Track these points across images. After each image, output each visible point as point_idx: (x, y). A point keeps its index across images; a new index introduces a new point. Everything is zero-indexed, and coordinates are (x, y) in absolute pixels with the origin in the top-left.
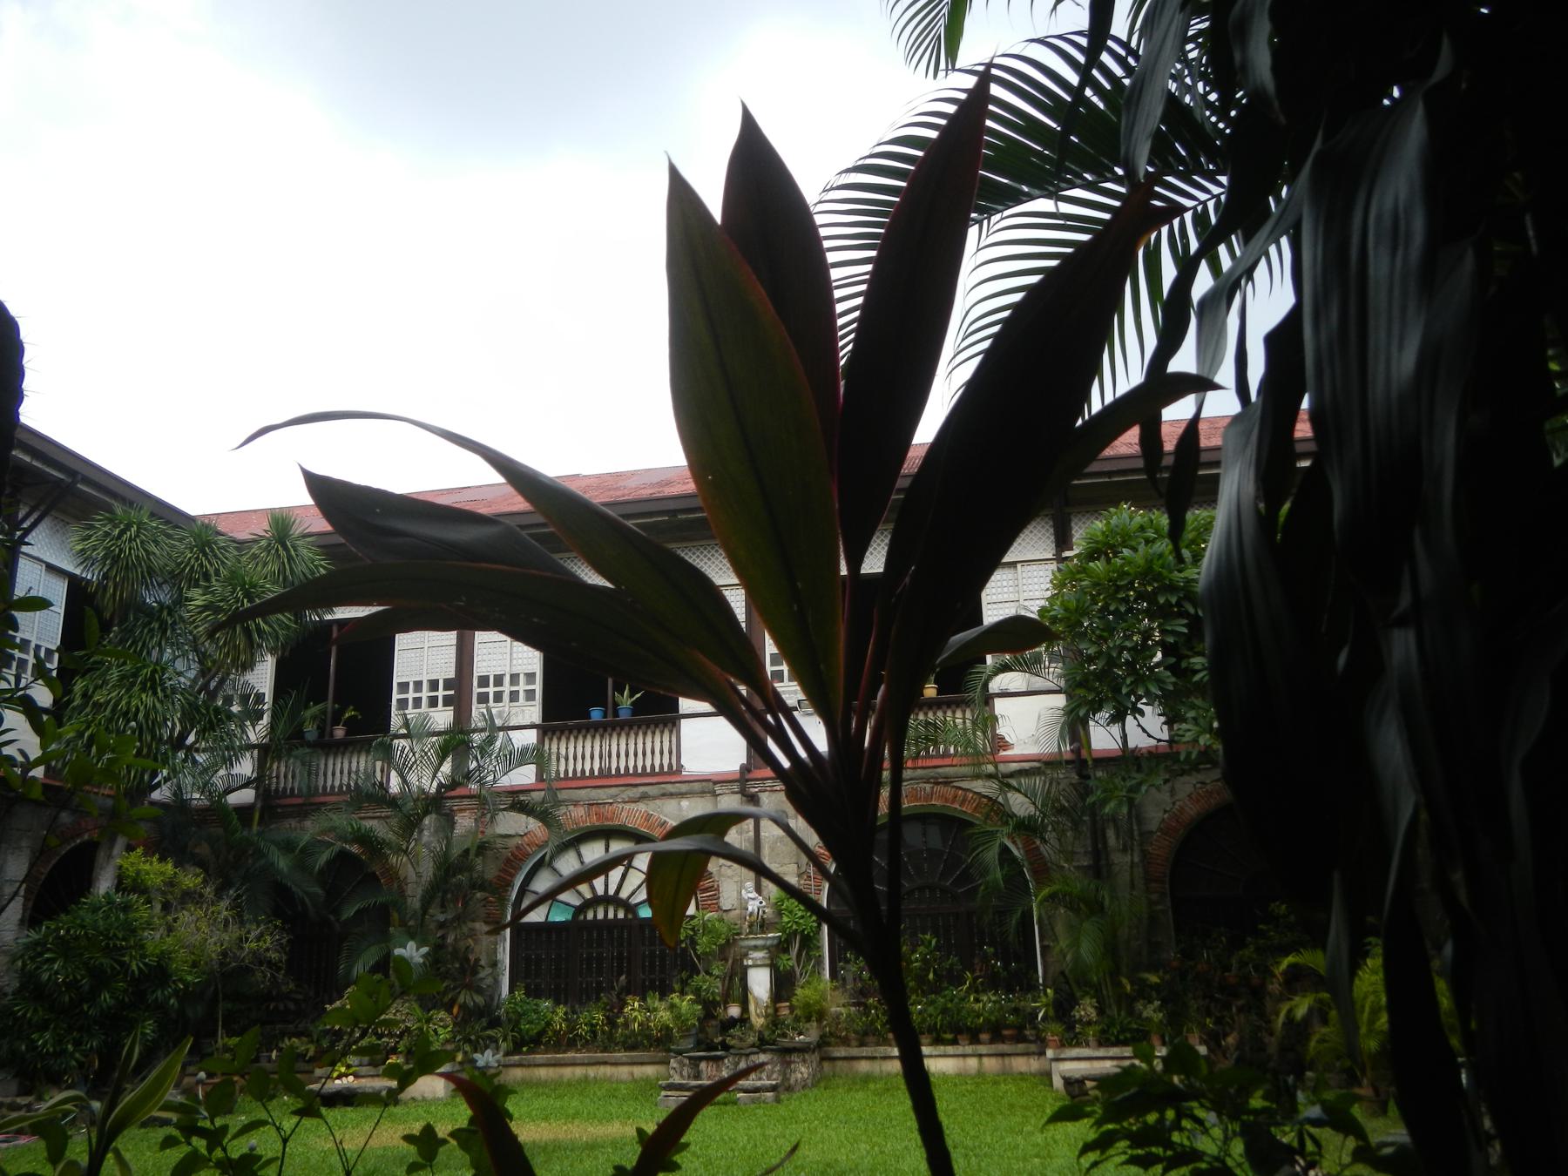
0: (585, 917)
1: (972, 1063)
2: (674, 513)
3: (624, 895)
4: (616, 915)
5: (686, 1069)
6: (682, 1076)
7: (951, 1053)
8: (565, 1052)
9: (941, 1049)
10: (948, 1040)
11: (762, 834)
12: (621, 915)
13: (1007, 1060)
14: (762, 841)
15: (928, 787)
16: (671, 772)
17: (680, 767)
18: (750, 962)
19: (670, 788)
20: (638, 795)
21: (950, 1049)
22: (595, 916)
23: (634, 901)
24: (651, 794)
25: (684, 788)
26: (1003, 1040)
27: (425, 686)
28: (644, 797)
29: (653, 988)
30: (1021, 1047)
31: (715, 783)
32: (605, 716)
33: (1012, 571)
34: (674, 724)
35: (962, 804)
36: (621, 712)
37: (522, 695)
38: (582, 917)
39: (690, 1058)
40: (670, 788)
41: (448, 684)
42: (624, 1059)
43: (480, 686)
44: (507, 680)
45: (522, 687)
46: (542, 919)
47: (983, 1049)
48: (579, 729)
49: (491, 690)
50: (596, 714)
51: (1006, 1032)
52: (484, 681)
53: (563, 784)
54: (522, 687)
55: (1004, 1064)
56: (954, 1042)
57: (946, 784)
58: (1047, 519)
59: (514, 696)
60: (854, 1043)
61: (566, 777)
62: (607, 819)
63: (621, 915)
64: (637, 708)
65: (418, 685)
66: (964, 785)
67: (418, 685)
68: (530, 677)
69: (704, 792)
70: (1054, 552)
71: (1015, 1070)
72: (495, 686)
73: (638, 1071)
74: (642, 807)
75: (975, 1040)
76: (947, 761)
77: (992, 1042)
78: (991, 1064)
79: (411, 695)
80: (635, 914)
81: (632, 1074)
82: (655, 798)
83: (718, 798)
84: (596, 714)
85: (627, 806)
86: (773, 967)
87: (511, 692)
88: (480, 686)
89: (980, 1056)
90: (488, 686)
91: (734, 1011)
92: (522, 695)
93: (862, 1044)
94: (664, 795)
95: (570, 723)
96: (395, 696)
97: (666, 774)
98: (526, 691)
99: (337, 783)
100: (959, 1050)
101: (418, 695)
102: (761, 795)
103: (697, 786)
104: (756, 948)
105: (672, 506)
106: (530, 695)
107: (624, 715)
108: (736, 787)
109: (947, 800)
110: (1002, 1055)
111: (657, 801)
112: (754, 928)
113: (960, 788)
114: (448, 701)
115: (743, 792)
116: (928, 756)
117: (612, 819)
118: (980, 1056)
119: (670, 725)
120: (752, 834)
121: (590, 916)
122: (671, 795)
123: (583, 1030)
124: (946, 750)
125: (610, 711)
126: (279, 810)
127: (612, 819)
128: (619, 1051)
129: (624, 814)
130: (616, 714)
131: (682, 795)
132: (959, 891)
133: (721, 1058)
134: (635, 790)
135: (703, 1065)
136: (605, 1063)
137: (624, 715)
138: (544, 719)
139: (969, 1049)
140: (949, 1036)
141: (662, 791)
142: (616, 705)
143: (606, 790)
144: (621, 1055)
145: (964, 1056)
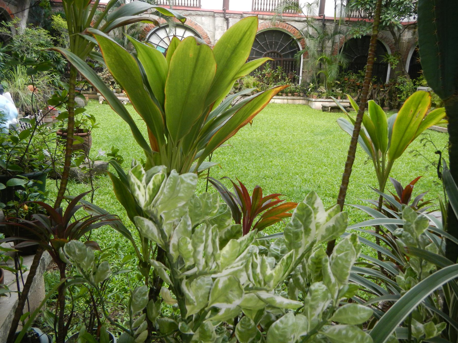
1: (286, 101)
16: (196, 7)
17: (200, 7)
19: (199, 13)
21: (281, 97)
25: (203, 13)
26: (294, 95)
30: (299, 98)
31: (215, 13)
35: (287, 29)
40: (199, 13)
47: (289, 97)
56: (282, 95)
69: (210, 15)
76: (289, 15)
77: (291, 96)
78: (290, 101)
82: (193, 15)
94: (196, 15)
99: (273, 8)
100: (283, 97)
103: (208, 13)
108: (222, 15)
115: (225, 17)
116: (288, 13)
122: (199, 15)
124: (291, 11)
126: (54, 4)
131: (203, 15)
134: (187, 12)
139: (286, 97)
143: (178, 11)
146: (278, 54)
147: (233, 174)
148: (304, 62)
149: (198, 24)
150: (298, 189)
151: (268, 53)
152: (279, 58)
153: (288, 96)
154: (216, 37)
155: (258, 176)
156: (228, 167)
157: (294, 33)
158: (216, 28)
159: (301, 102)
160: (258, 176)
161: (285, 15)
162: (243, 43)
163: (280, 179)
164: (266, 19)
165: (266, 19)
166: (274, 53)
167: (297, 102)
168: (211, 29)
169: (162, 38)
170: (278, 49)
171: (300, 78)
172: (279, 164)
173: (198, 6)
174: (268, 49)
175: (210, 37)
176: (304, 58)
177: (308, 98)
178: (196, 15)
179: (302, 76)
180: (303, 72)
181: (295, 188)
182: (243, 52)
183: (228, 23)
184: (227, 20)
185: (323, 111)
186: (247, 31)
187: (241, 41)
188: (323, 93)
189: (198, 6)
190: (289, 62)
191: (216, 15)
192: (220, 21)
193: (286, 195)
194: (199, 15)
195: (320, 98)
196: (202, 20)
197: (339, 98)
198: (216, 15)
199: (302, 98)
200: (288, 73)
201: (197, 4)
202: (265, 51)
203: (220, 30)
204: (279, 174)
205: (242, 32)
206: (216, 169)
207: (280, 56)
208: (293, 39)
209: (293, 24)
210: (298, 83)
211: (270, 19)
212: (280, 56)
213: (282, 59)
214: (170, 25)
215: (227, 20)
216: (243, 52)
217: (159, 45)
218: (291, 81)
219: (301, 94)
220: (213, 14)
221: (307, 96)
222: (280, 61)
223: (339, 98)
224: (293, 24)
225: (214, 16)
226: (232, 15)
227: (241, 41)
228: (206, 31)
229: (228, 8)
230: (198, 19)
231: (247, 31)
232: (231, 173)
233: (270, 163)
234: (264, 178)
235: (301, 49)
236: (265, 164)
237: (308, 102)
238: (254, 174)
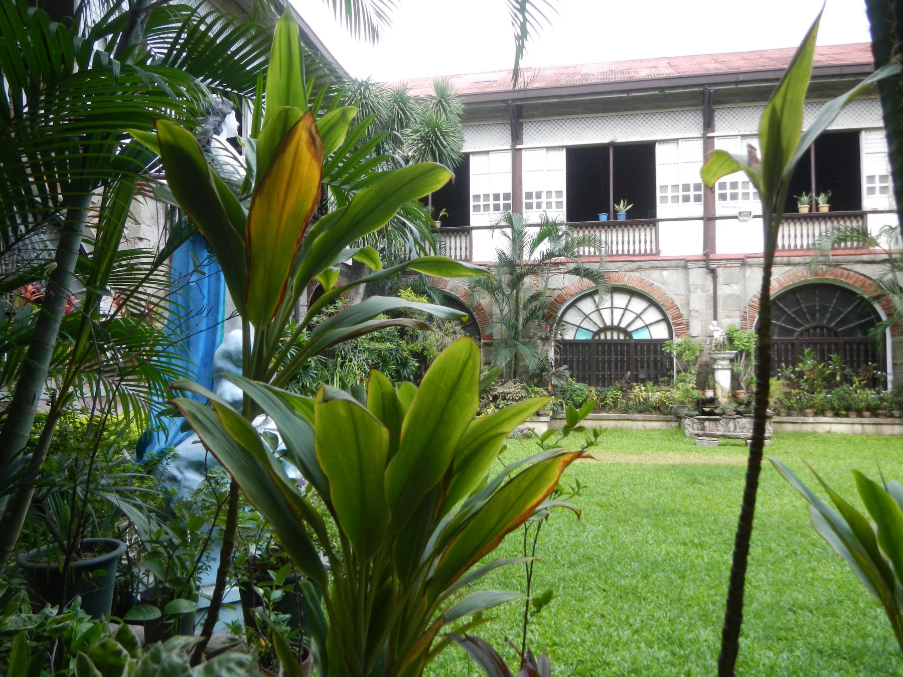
0: (600, 338)
1: (858, 428)
2: (662, 89)
3: (623, 325)
4: (619, 337)
5: (696, 425)
6: (693, 428)
8: (599, 413)
9: (839, 419)
11: (718, 293)
12: (622, 337)
13: (879, 427)
14: (718, 297)
15: (824, 267)
16: (651, 254)
17: (658, 252)
18: (720, 367)
19: (657, 264)
20: (635, 267)
21: (845, 420)
22: (606, 337)
23: (629, 329)
24: (644, 266)
25: (665, 264)
26: (877, 416)
27: (491, 197)
28: (639, 269)
29: (649, 379)
30: (889, 420)
31: (688, 261)
32: (608, 219)
33: (675, 145)
34: (468, 233)
36: (619, 217)
37: (554, 205)
38: (597, 338)
39: (698, 419)
41: (697, 187)
42: (640, 418)
43: (527, 198)
44: (544, 195)
45: (692, 193)
46: (572, 338)
47: (865, 420)
48: (793, 219)
49: (534, 201)
50: (603, 217)
51: (881, 412)
52: (529, 195)
53: (586, 260)
54: (554, 199)
56: (847, 416)
57: (836, 266)
58: (698, 112)
59: (549, 205)
60: (783, 414)
61: (617, 255)
62: (615, 281)
63: (622, 337)
64: (629, 214)
65: (539, 195)
66: (848, 267)
67: (486, 196)
68: (559, 193)
69: (677, 267)
70: (702, 132)
72: (537, 198)
73: (648, 425)
74: (637, 274)
75: (860, 414)
76: (847, 252)
77: (871, 416)
78: (870, 429)
79: (482, 203)
80: (631, 337)
81: (644, 427)
82: (646, 269)
83: (690, 270)
84: (603, 217)
85: (628, 274)
86: (732, 370)
87: (547, 203)
88: (527, 198)
89: (863, 424)
90: (689, 191)
91: (709, 394)
92: (554, 205)
93: (789, 415)
94: (652, 268)
95: (587, 222)
96: (472, 203)
97: (593, 256)
98: (557, 202)
101: (549, 200)
102: (718, 269)
103: (674, 263)
104: (724, 359)
105: (664, 84)
106: (559, 204)
107: (622, 218)
108: (702, 264)
109: (836, 276)
110: (876, 424)
111: (648, 272)
112: (719, 347)
113: (845, 269)
114: (697, 199)
115: (707, 267)
116: (846, 248)
117: (618, 281)
118: (863, 424)
119: (651, 225)
120: (711, 292)
121: (602, 337)
122: (657, 267)
123: (609, 401)
124: (852, 245)
125: (612, 216)
127: (618, 281)
128: (633, 413)
129: (626, 278)
130: (616, 217)
131: (663, 268)
132: (839, 330)
133: (718, 420)
134: (634, 264)
135: (707, 423)
136: (628, 420)
137: (622, 218)
138: (567, 221)
139: (857, 420)
140: (844, 413)
141: (651, 265)
142: (616, 212)
144: (637, 416)
145: (853, 424)
146: (829, 330)
147: (716, 595)
149: (656, 284)
150: (878, 644)
151: (808, 330)
152: (833, 339)
154: (691, 305)
155: (777, 603)
156: (707, 578)
157: (863, 286)
158: (692, 288)
160: (777, 603)
161: (838, 252)
162: (465, 381)
163: (834, 615)
164: (795, 265)
165: (795, 265)
166: (822, 328)
167: (888, 430)
168: (682, 290)
169: (587, 313)
170: (831, 320)
171: (890, 378)
172: (832, 577)
173: (654, 251)
174: (807, 322)
175: (679, 306)
176: (892, 336)
178: (652, 268)
179: (894, 374)
180: (894, 365)
181: (870, 641)
182: (468, 395)
183: (715, 278)
184: (713, 272)
186: (468, 359)
187: (460, 376)
189: (654, 251)
190: (859, 344)
191: (690, 265)
192: (698, 275)
193: (845, 659)
194: (657, 267)
196: (662, 276)
198: (690, 265)
199: (897, 421)
200: (859, 367)
201: (651, 249)
202: (799, 325)
203: (699, 291)
204: (830, 602)
205: (461, 362)
206: (679, 581)
207: (836, 334)
208: (863, 299)
209: (859, 268)
210: (886, 388)
211: (805, 264)
212: (836, 334)
213: (841, 340)
214: (601, 289)
215: (713, 272)
216: (468, 395)
217: (582, 325)
218: (867, 385)
220: (684, 264)
222: (836, 344)
224: (859, 268)
225: (686, 268)
226: (723, 262)
227: (460, 376)
228: (671, 295)
229: (713, 251)
230: (656, 274)
231: (468, 359)
232: (712, 592)
233: (811, 574)
234: (790, 610)
235: (884, 317)
236: (795, 575)
238: (768, 599)
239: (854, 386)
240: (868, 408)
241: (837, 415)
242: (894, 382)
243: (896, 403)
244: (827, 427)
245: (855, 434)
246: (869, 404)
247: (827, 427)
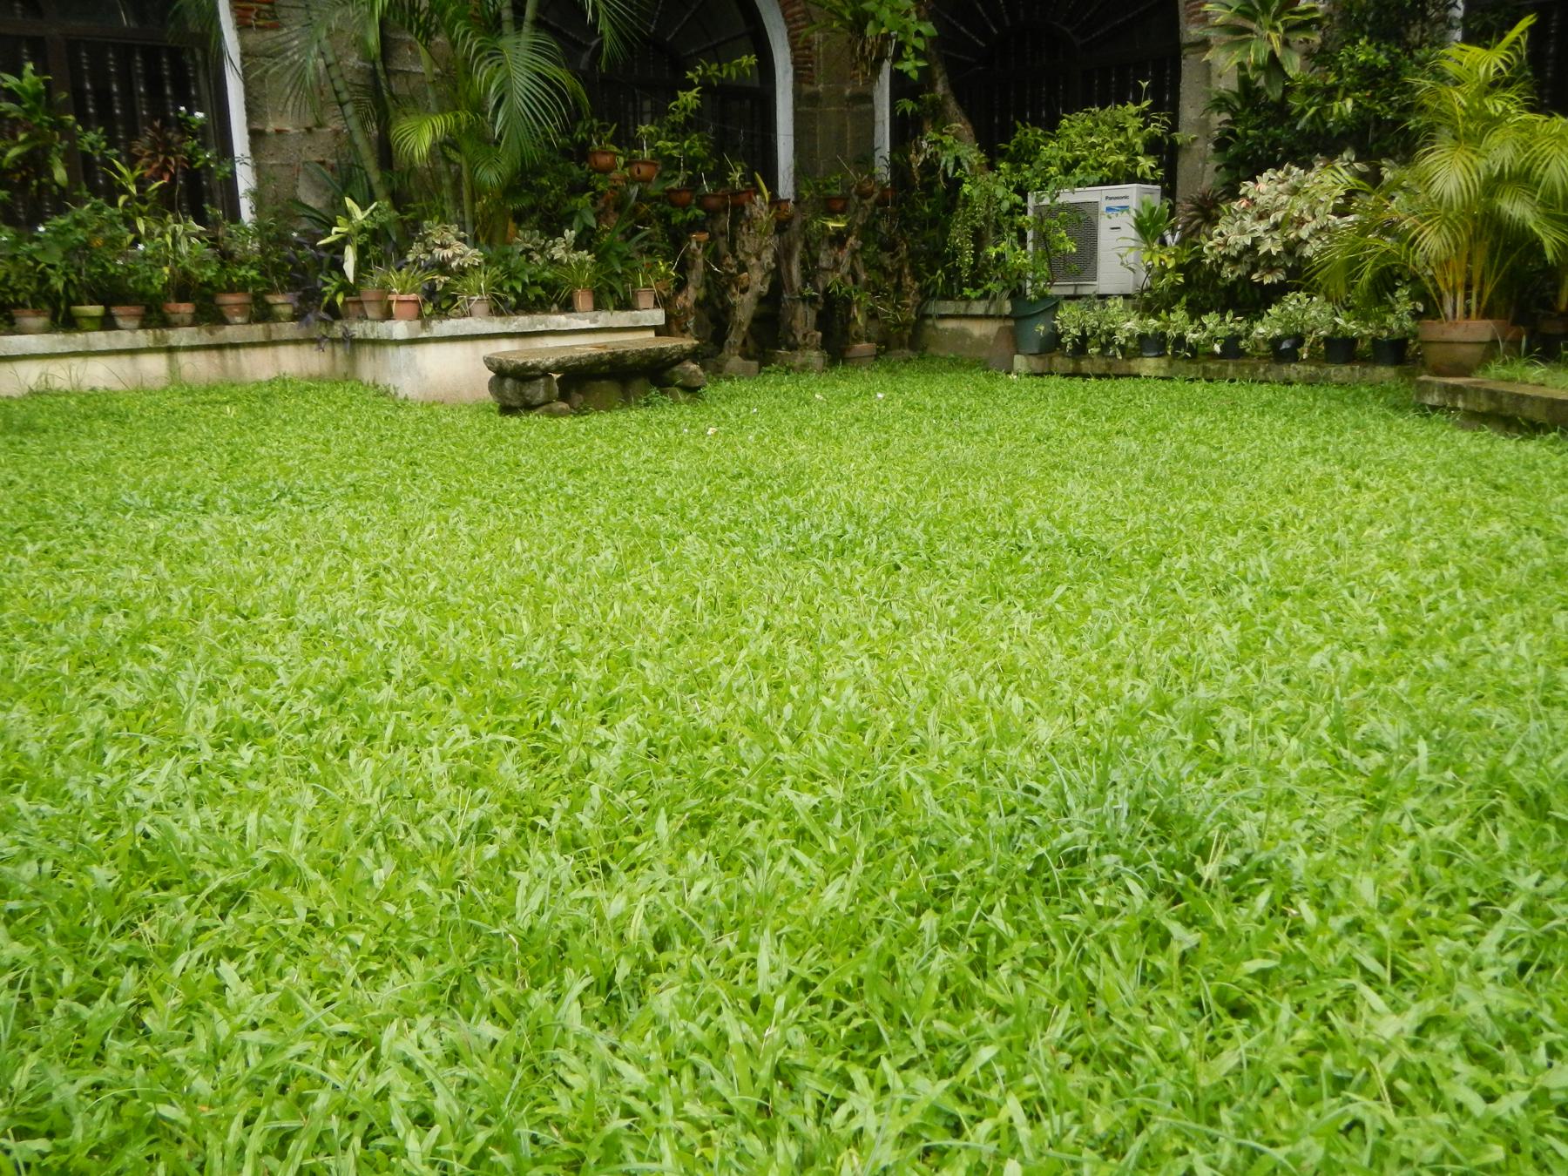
1: (154, 366)
7: (103, 346)
9: (77, 340)
10: (91, 318)
13: (229, 354)
21: (100, 339)
47: (179, 336)
55: (224, 368)
56: (107, 323)
71: (248, 377)
75: (154, 316)
77: (195, 322)
78: (197, 366)
89: (171, 350)
100: (124, 339)
110: (220, 347)
140: (96, 310)
145: (133, 352)
148: (245, 54)
153: (167, 323)
159: (293, 361)
167: (259, 365)
171: (245, 179)
176: (242, 26)
177: (338, 329)
179: (258, 169)
180: (256, 136)
185: (507, 410)
188: (462, 272)
195: (442, 313)
197: (583, 299)
199: (288, 329)
200: (133, 134)
210: (235, 216)
219: (282, 302)
221: (334, 312)
223: (583, 299)
237: (352, 358)
239: (122, 200)
240: (183, 288)
241: (69, 324)
242: (257, 196)
243: (277, 269)
244: (30, 374)
245: (141, 389)
246: (186, 273)
247: (30, 374)
